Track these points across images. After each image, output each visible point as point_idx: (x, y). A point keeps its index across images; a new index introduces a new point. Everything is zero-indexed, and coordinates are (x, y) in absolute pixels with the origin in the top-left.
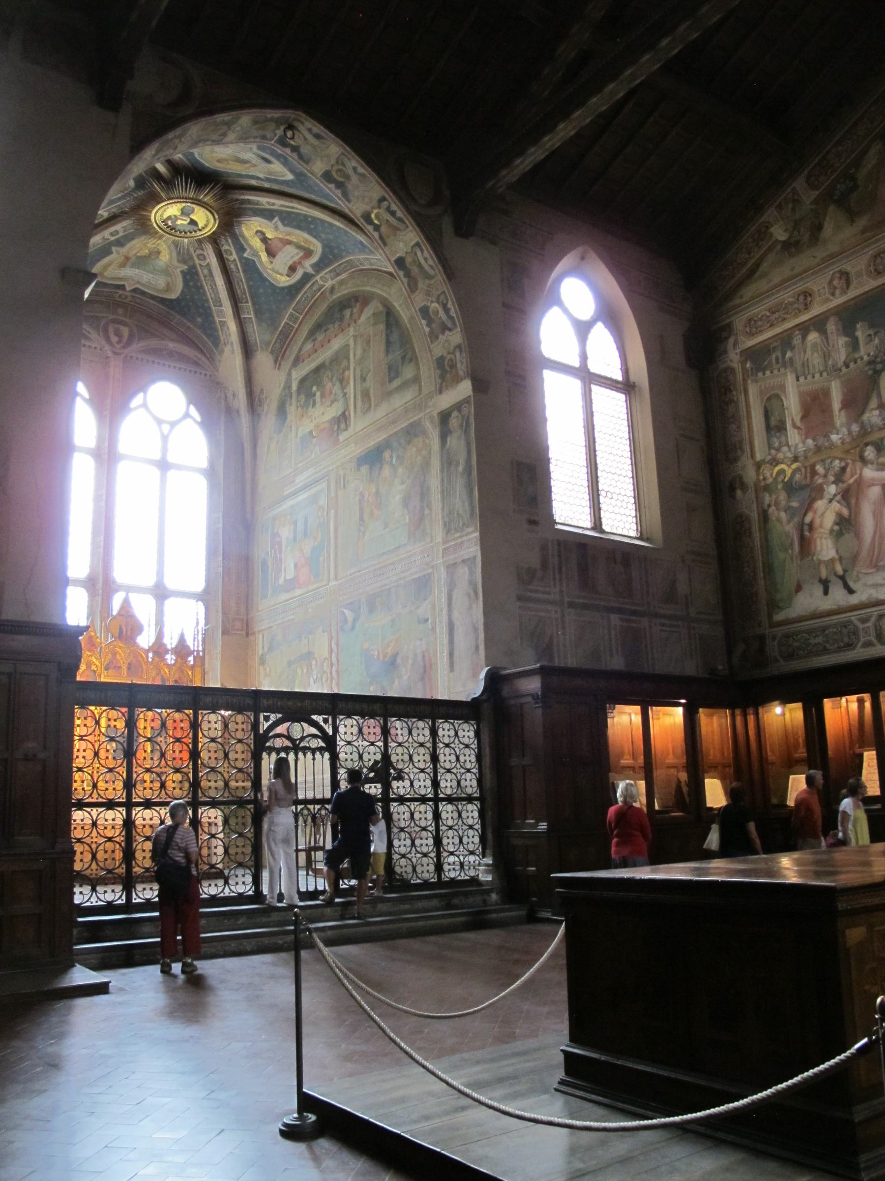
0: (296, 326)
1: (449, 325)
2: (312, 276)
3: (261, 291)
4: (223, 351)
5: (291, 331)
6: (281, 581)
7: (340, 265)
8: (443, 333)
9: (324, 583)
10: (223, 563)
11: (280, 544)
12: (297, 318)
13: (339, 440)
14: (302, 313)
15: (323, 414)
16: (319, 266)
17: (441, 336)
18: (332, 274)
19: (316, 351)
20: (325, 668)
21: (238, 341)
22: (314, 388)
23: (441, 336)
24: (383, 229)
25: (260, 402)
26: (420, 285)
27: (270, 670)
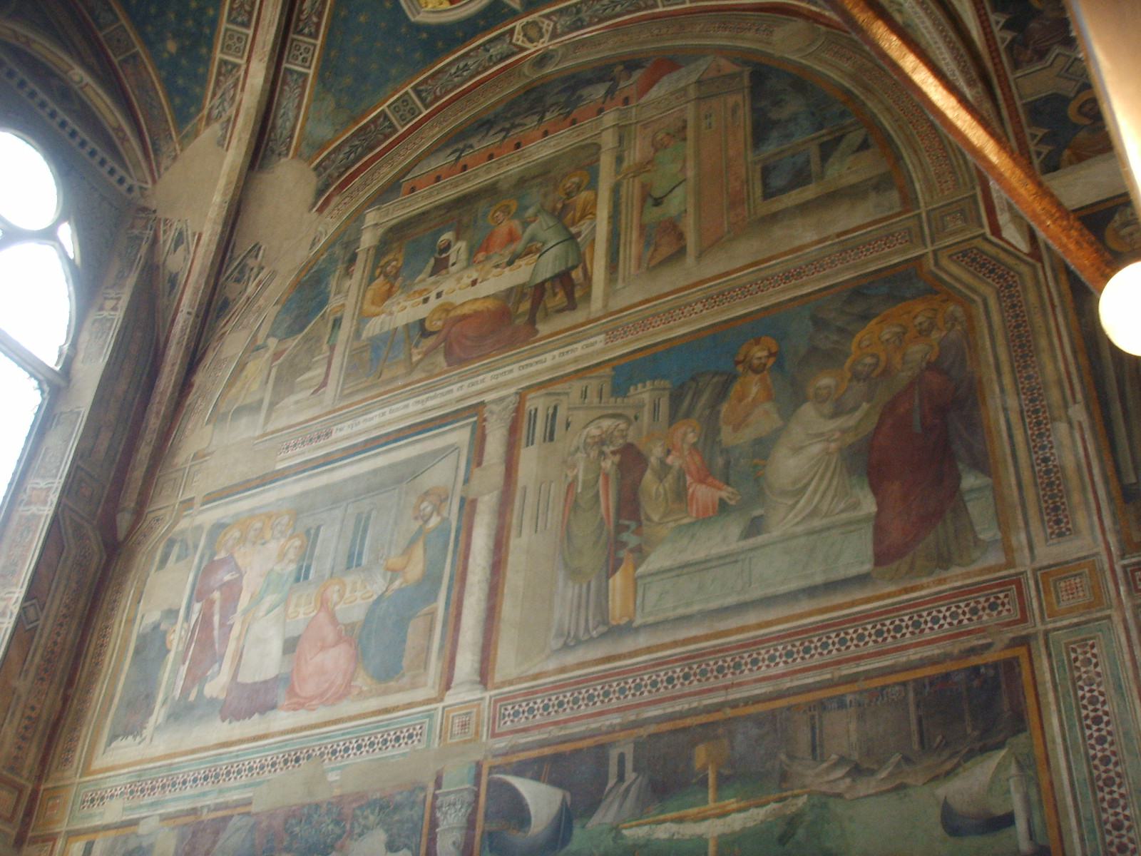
0: (402, 131)
2: (514, 15)
3: (362, 19)
4: (196, 134)
5: (387, 137)
6: (216, 686)
9: (420, 694)
10: (23, 610)
11: (232, 592)
12: (414, 112)
13: (537, 332)
14: (432, 103)
15: (474, 283)
18: (566, 20)
19: (465, 168)
21: (253, 112)
22: (447, 236)
23: (1057, 50)
25: (242, 272)
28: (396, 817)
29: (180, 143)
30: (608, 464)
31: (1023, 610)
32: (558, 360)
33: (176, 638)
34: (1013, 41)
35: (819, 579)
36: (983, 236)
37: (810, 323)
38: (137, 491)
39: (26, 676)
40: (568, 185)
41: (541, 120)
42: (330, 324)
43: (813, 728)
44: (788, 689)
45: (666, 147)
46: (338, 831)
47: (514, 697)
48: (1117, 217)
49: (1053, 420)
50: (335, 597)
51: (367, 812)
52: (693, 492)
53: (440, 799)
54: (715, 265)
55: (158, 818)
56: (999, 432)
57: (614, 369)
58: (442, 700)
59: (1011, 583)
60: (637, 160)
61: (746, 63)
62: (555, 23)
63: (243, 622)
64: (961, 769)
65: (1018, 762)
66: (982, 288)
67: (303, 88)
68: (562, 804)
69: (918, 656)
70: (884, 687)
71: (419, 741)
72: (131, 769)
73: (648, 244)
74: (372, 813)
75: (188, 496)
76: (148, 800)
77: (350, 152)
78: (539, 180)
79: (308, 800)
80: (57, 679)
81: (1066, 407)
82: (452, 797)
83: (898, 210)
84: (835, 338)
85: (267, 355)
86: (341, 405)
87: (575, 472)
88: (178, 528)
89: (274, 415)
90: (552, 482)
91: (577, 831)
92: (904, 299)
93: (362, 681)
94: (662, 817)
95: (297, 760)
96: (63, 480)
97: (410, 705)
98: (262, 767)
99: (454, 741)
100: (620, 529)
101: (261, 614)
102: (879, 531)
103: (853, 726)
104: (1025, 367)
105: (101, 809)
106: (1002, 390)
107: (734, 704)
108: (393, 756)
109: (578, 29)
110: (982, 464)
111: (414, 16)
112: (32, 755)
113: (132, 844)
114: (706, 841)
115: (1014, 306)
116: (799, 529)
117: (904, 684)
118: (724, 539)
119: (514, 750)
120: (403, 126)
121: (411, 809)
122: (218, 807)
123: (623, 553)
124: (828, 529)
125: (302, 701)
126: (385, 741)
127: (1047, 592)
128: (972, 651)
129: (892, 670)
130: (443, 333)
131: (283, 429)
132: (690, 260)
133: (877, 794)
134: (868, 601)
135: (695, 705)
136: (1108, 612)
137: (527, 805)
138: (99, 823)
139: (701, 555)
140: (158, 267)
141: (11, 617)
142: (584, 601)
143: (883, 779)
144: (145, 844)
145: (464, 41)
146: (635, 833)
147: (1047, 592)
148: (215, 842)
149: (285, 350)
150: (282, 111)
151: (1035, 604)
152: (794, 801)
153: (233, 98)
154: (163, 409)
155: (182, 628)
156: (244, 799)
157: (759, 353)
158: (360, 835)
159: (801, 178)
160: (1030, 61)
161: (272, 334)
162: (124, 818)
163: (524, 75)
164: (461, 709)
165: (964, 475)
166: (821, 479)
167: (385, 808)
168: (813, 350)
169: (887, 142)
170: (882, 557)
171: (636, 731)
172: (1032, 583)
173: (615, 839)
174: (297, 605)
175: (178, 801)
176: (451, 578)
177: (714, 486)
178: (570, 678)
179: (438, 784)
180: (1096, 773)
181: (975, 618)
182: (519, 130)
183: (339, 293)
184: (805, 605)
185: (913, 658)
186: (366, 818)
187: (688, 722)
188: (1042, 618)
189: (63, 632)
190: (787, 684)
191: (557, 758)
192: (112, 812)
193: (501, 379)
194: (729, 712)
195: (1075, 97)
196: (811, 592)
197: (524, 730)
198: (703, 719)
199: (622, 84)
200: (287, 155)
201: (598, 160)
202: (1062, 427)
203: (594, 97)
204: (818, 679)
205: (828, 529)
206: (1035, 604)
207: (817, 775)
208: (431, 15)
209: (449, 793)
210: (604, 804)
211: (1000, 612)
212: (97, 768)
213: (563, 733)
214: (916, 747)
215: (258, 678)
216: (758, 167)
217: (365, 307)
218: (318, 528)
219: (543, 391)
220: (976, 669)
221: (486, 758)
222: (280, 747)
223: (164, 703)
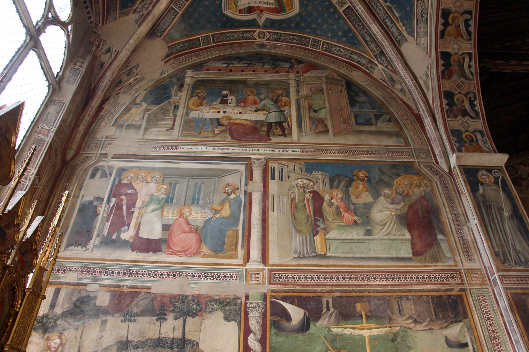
0: (202, 47)
1: (472, 114)
2: (259, 27)
4: (128, 14)
5: (196, 47)
6: (127, 235)
7: (290, 35)
8: (464, 116)
12: (209, 43)
14: (216, 42)
15: (240, 113)
16: (271, 24)
17: (460, 117)
18: (275, 37)
23: (460, 117)
24: (449, 28)
25: (130, 73)
26: (455, 77)
27: (62, 344)
29: (119, 15)
30: (308, 196)
31: (462, 281)
32: (281, 152)
33: (102, 210)
34: (448, 109)
35: (394, 256)
36: (433, 162)
37: (379, 171)
38: (77, 143)
40: (278, 92)
41: (263, 66)
42: (173, 107)
43: (399, 304)
44: (388, 290)
45: (316, 94)
48: (480, 172)
49: (463, 225)
50: (187, 214)
52: (344, 215)
53: (248, 304)
54: (340, 140)
56: (447, 224)
57: (305, 163)
58: (245, 266)
59: (458, 271)
60: (305, 94)
61: (344, 78)
62: (271, 36)
63: (139, 212)
64: (449, 327)
65: (467, 327)
66: (435, 178)
67: (175, 17)
68: (304, 315)
69: (431, 288)
70: (421, 296)
71: (236, 279)
73: (313, 124)
74: (216, 304)
75: (104, 152)
76: (91, 276)
77: (182, 47)
78: (265, 86)
81: (466, 222)
83: (404, 145)
84: (388, 178)
85: (142, 109)
86: (182, 139)
87: (294, 195)
88: (99, 164)
89: (147, 133)
90: (284, 196)
91: (312, 326)
92: (410, 173)
94: (346, 326)
96: (56, 129)
100: (316, 220)
101: (149, 211)
102: (413, 245)
103: (412, 306)
104: (452, 207)
105: (63, 275)
106: (446, 212)
107: (369, 291)
109: (277, 41)
110: (443, 233)
111: (225, 11)
113: (84, 294)
115: (445, 187)
116: (385, 237)
117: (427, 296)
118: (358, 234)
120: (203, 46)
121: (235, 306)
122: (132, 287)
123: (318, 229)
124: (396, 240)
127: (469, 277)
128: (448, 290)
129: (423, 291)
130: (228, 127)
131: (153, 140)
132: (331, 135)
133: (423, 330)
134: (412, 266)
135: (354, 289)
136: (487, 287)
137: (289, 313)
139: (349, 237)
140: (97, 57)
141: (30, 181)
142: (305, 242)
144: (91, 295)
145: (237, 27)
146: (336, 330)
147: (469, 277)
149: (150, 110)
150: (164, 21)
151: (465, 280)
152: (395, 328)
153: (148, 8)
154: (92, 113)
155: (105, 206)
157: (361, 175)
158: (210, 312)
159: (368, 122)
160: (452, 117)
161: (144, 100)
162: (78, 282)
163: (254, 47)
165: (438, 235)
166: (391, 222)
168: (381, 180)
169: (397, 122)
170: (415, 253)
172: (463, 273)
174: (167, 212)
176: (244, 219)
177: (351, 215)
178: (303, 269)
179: (247, 297)
181: (448, 280)
182: (253, 66)
183: (176, 96)
184: (390, 263)
185: (429, 288)
186: (213, 305)
187: (352, 294)
188: (468, 284)
190: (388, 288)
192: (72, 277)
193: (257, 152)
194: (367, 294)
195: (465, 132)
196: (392, 259)
198: (358, 294)
199: (295, 66)
200: (160, 37)
201: (289, 88)
202: (466, 228)
203: (284, 66)
204: (398, 289)
205: (396, 240)
206: (465, 280)
207: (402, 321)
208: (230, 13)
211: (455, 280)
214: (434, 317)
216: (353, 113)
217: (190, 105)
218: (175, 184)
219: (277, 162)
220: (450, 296)
222: (165, 269)
223: (98, 236)
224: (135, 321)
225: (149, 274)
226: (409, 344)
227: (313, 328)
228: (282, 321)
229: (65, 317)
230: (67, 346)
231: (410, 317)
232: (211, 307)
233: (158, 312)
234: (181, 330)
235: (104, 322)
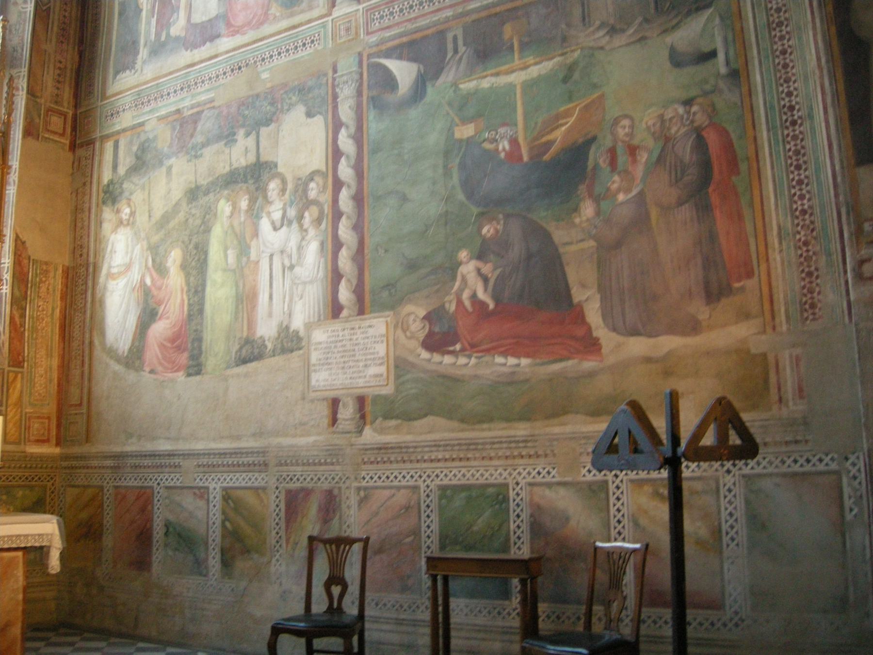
6: (178, 28)
9: (315, 13)
20: (312, 194)
27: (133, 214)
28: (310, 95)
39: (51, 41)
46: (273, 109)
47: (380, 6)
51: (291, 95)
53: (337, 80)
55: (156, 119)
58: (330, 15)
64: (682, 24)
68: (418, 73)
71: (319, 44)
72: (132, 91)
74: (294, 95)
76: (147, 109)
79: (251, 93)
80: (71, 41)
82: (345, 78)
91: (430, 90)
93: (275, 10)
94: (485, 73)
95: (240, 68)
97: (309, 21)
98: (217, 76)
99: (342, 40)
105: (118, 120)
108: (302, 57)
112: (67, 93)
113: (143, 137)
114: (515, 86)
119: (382, 42)
122: (192, 107)
125: (237, 29)
126: (296, 48)
137: (395, 76)
138: (119, 128)
143: (630, 35)
144: (151, 136)
148: (195, 129)
156: (208, 99)
158: (288, 110)
162: (134, 123)
164: (344, 19)
167: (302, 91)
171: (464, 19)
173: (455, 91)
175: (166, 107)
179: (335, 71)
180: (771, 19)
186: (290, 99)
189: (68, 9)
191: (412, 43)
197: (388, 27)
209: (342, 76)
210: (446, 70)
212: (111, 93)
213: (414, 26)
214: (652, 11)
215: (204, 19)
221: (364, 49)
222: (227, 62)
223: (145, 45)
224: (201, 155)
225: (210, 79)
226: (595, 81)
227: (431, 91)
228: (384, 93)
229: (130, 177)
230: (137, 214)
231: (602, 25)
232: (289, 102)
233: (226, 133)
234: (255, 151)
235: (170, 168)
